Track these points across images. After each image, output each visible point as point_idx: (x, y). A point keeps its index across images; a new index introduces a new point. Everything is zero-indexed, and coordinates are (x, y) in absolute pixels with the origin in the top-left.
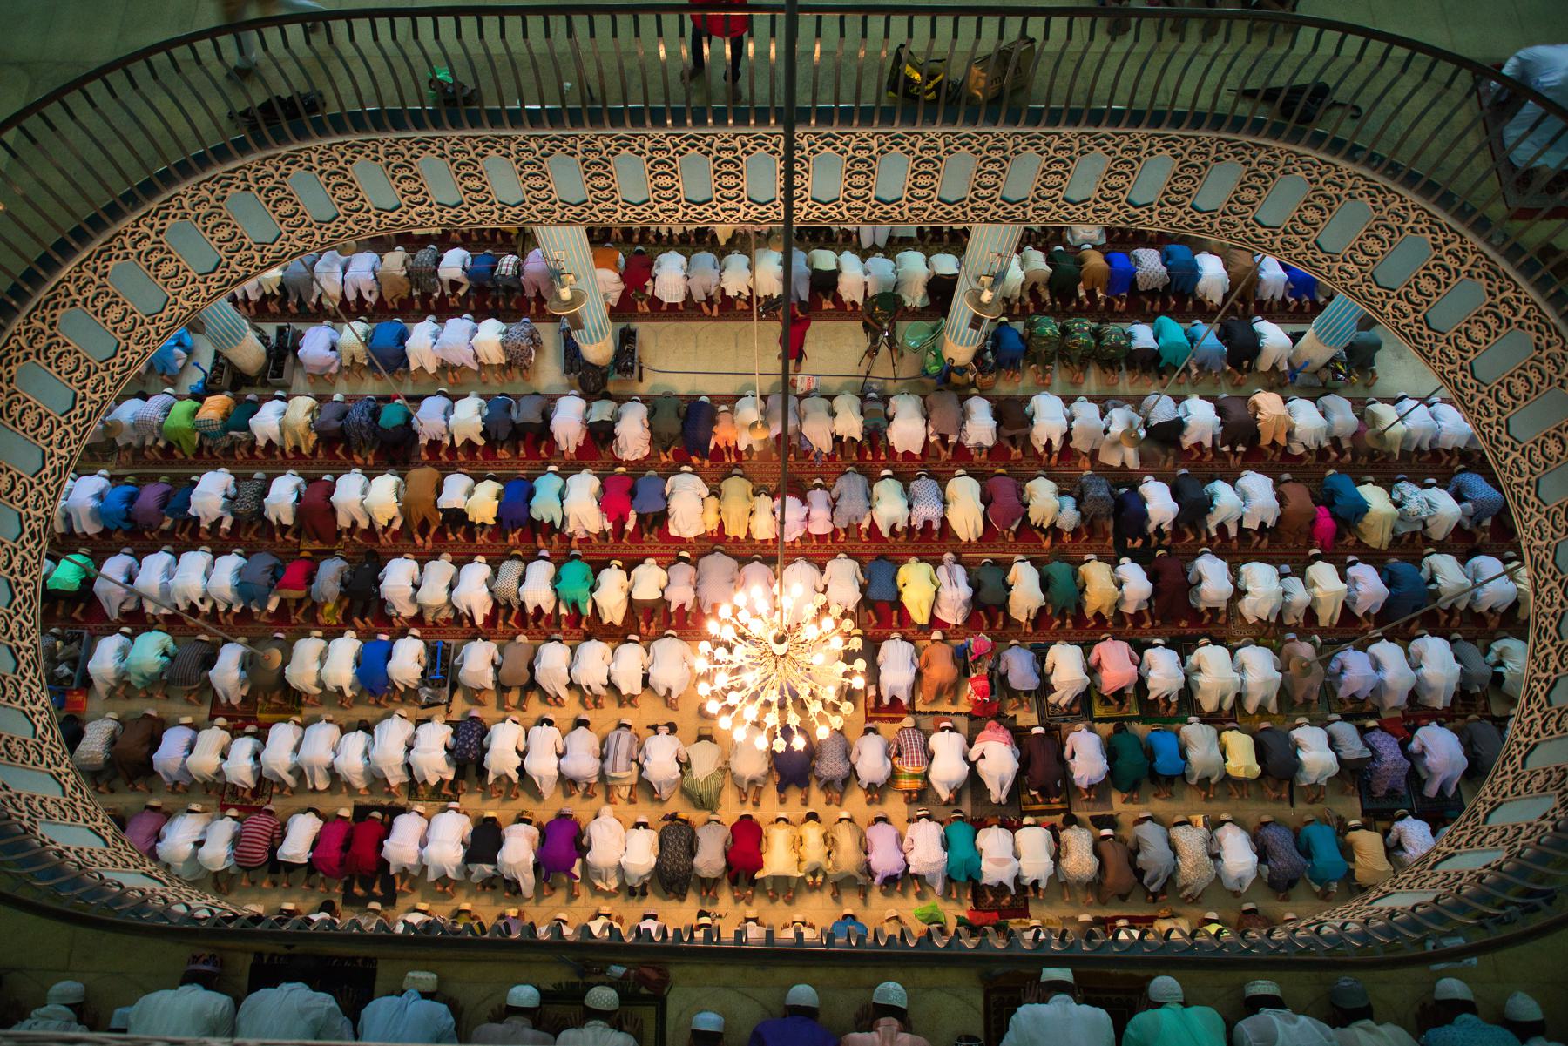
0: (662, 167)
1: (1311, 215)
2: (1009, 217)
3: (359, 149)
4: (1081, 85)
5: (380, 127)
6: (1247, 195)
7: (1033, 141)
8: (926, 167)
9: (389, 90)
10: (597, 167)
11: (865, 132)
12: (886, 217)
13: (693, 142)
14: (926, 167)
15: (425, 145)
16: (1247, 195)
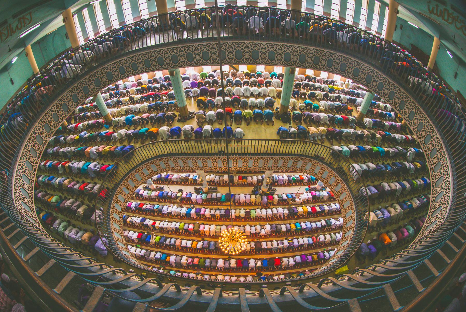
0: (215, 162)
1: (313, 168)
2: (269, 170)
3: (169, 159)
4: (278, 150)
5: (173, 156)
6: (304, 165)
7: (272, 158)
8: (256, 162)
9: (174, 150)
10: (205, 162)
11: (246, 157)
12: (250, 169)
13: (219, 158)
14: (256, 162)
15: (179, 158)
16: (304, 165)
